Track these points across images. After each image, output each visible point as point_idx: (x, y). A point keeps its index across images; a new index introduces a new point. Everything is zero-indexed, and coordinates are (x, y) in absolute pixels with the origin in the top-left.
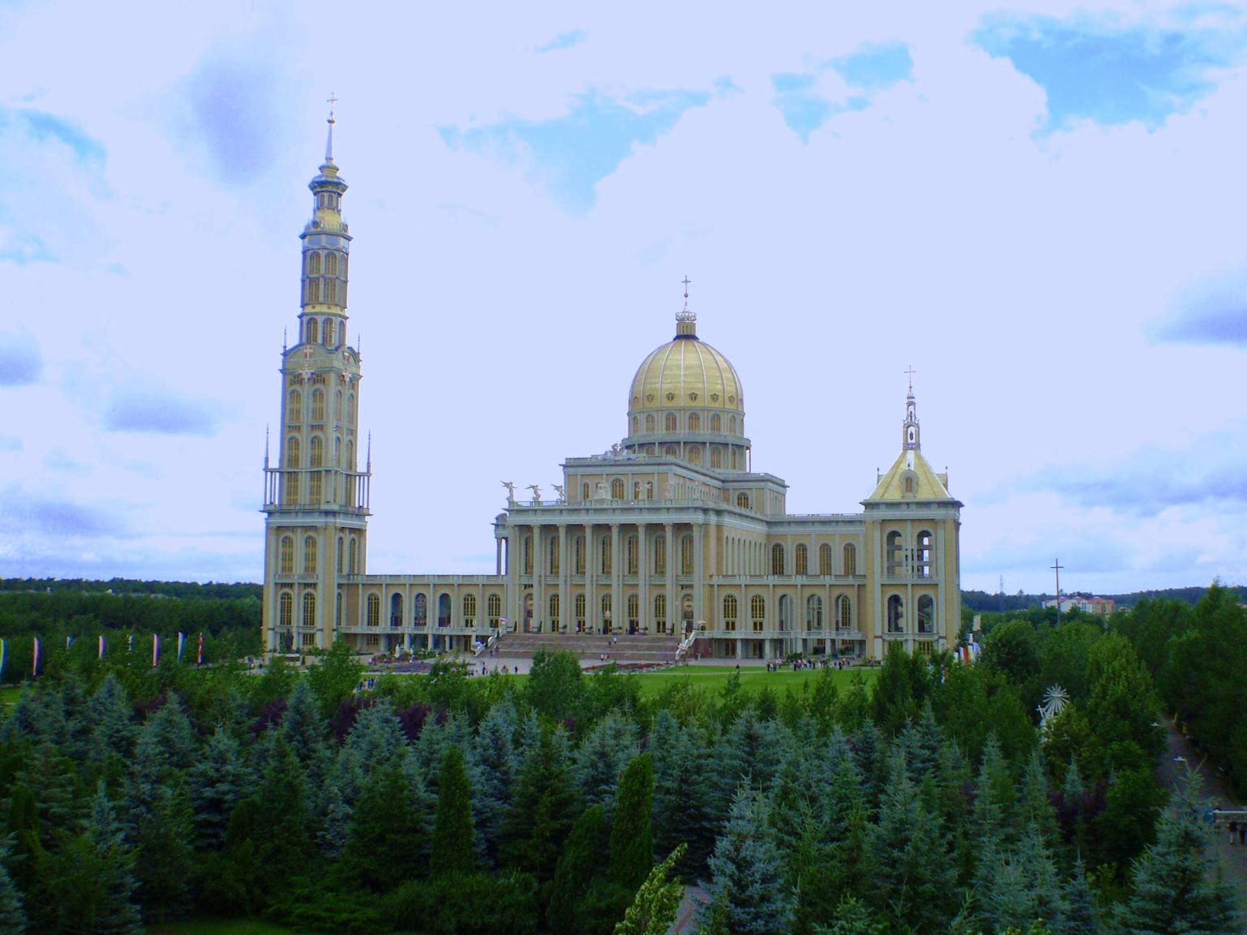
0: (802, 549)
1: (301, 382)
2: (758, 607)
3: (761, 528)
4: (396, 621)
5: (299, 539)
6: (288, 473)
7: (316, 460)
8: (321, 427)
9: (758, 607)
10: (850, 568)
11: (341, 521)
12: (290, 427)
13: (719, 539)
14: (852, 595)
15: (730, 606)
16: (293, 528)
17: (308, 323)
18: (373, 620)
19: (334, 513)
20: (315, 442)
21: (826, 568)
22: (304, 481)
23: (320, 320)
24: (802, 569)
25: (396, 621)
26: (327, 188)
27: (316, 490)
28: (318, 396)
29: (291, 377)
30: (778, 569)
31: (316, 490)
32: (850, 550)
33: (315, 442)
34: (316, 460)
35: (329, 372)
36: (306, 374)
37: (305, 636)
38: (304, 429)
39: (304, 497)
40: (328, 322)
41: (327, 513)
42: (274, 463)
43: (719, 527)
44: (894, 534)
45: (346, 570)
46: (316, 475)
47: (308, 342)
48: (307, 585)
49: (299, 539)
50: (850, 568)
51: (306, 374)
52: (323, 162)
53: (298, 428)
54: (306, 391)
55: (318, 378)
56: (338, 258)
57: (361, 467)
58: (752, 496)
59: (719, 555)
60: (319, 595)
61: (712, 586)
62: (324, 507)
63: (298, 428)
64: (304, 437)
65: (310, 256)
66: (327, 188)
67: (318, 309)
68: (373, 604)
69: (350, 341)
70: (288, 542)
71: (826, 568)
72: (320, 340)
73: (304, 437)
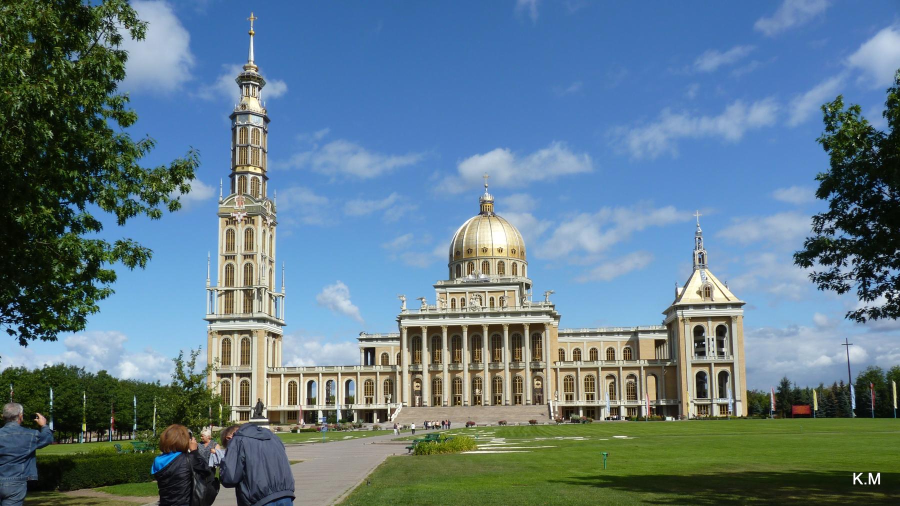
4: (311, 401)
5: (236, 341)
7: (248, 280)
8: (252, 257)
16: (231, 332)
18: (293, 400)
19: (264, 320)
20: (248, 269)
22: (239, 298)
28: (249, 233)
33: (248, 269)
35: (257, 215)
36: (239, 217)
37: (241, 413)
38: (239, 258)
45: (270, 365)
48: (241, 375)
49: (236, 341)
53: (233, 257)
54: (240, 231)
55: (249, 219)
61: (555, 370)
62: (256, 315)
63: (233, 257)
64: (239, 265)
68: (293, 388)
70: (226, 344)
72: (249, 192)
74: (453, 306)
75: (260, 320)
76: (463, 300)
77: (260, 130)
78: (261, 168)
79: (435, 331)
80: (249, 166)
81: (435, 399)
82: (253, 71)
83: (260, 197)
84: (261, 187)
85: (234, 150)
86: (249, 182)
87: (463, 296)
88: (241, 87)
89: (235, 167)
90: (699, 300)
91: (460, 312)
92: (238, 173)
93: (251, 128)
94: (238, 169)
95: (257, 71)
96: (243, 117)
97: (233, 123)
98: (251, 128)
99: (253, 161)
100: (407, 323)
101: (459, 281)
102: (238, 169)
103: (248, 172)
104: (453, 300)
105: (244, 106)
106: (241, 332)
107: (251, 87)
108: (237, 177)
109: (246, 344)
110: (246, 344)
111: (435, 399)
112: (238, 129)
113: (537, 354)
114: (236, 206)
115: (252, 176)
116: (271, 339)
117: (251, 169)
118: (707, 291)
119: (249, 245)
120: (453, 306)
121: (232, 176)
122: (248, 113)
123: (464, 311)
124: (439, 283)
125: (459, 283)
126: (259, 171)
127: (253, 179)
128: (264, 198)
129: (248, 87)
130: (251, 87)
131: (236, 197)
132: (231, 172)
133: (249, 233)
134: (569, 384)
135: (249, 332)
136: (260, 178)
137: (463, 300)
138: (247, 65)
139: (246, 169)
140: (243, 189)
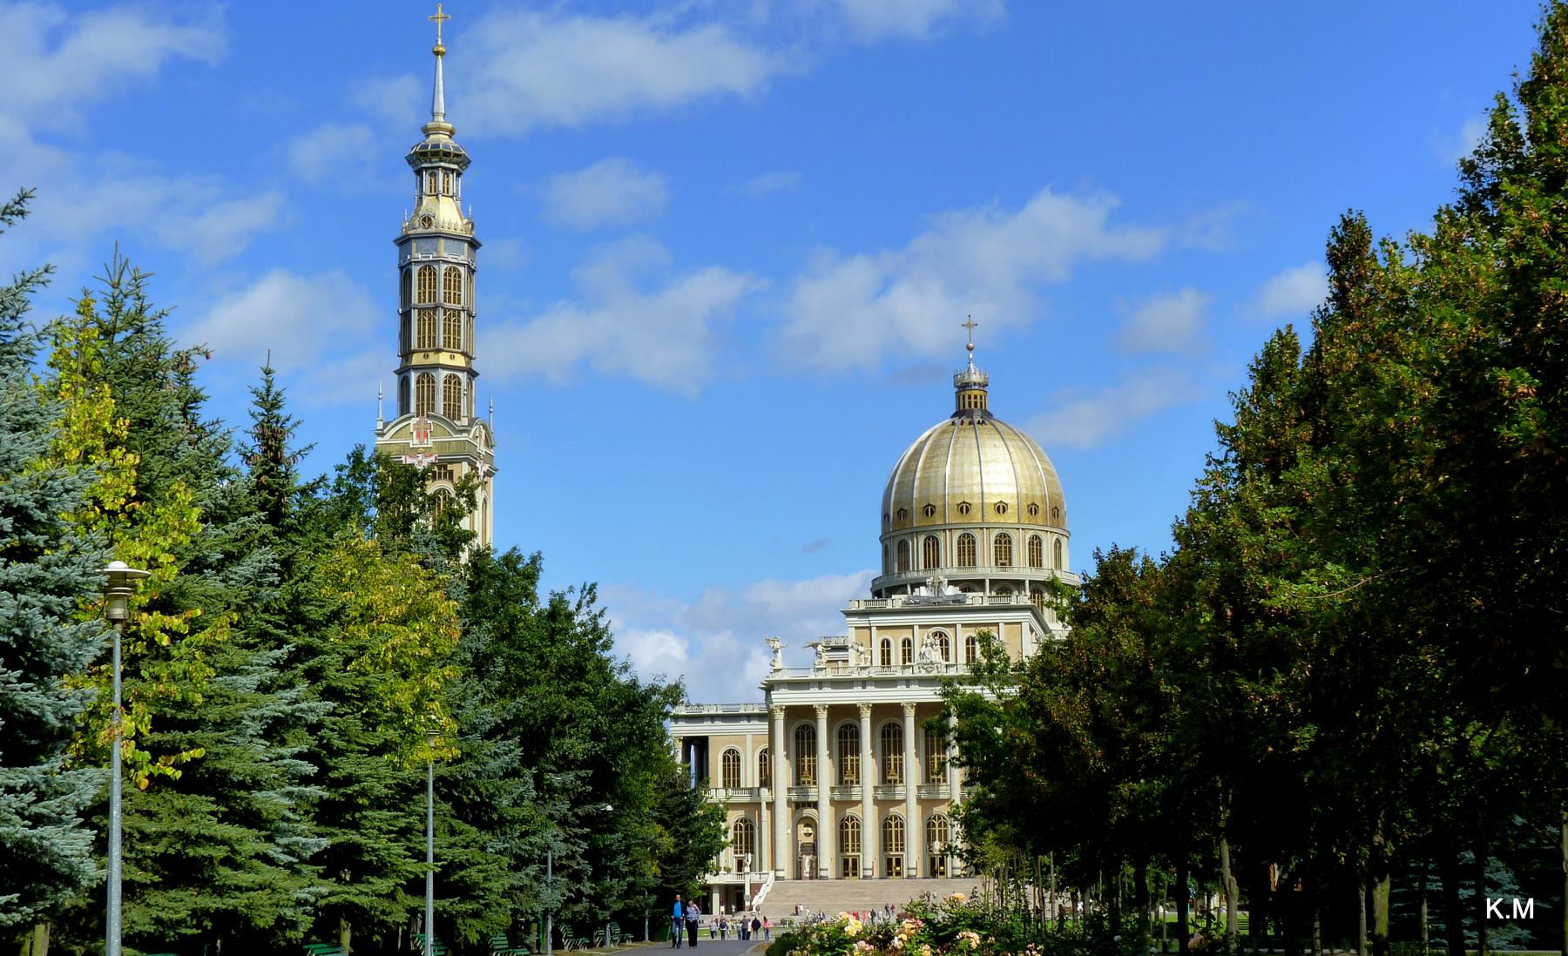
35: (459, 461)
72: (440, 410)
76: (907, 643)
77: (462, 269)
78: (463, 354)
79: (844, 717)
80: (439, 351)
81: (846, 862)
82: (443, 139)
83: (465, 421)
84: (464, 401)
85: (406, 317)
86: (440, 386)
87: (907, 634)
88: (419, 172)
89: (406, 354)
91: (899, 674)
92: (416, 368)
93: (444, 267)
94: (417, 359)
95: (451, 133)
96: (425, 244)
97: (402, 256)
98: (444, 267)
99: (447, 343)
100: (783, 698)
101: (897, 601)
102: (417, 359)
103: (437, 367)
104: (886, 644)
105: (427, 220)
107: (441, 174)
108: (414, 376)
111: (846, 862)
112: (415, 270)
114: (414, 442)
115: (445, 373)
117: (444, 358)
121: (403, 373)
122: (437, 236)
123: (908, 673)
124: (854, 607)
125: (898, 605)
126: (460, 361)
127: (448, 380)
128: (472, 422)
129: (433, 175)
130: (441, 174)
131: (414, 421)
132: (397, 363)
136: (463, 376)
137: (907, 643)
138: (430, 125)
139: (433, 359)
140: (427, 407)
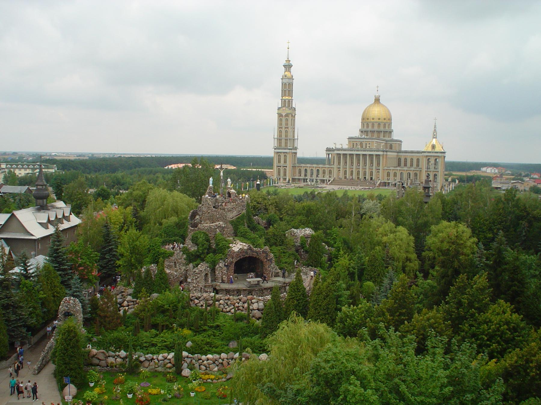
0: (406, 160)
1: (282, 116)
2: (395, 175)
3: (396, 154)
4: (305, 175)
6: (279, 140)
7: (286, 136)
9: (395, 175)
10: (418, 165)
11: (293, 151)
12: (280, 127)
13: (386, 158)
14: (418, 173)
15: (388, 174)
17: (284, 102)
19: (291, 149)
20: (286, 132)
21: (412, 165)
23: (287, 101)
24: (405, 165)
25: (305, 175)
26: (288, 67)
27: (286, 143)
28: (287, 120)
29: (280, 115)
30: (399, 165)
31: (286, 143)
32: (418, 160)
33: (286, 132)
34: (286, 136)
36: (284, 115)
38: (283, 128)
39: (283, 145)
40: (289, 101)
41: (290, 149)
42: (276, 137)
43: (386, 155)
44: (436, 159)
46: (286, 140)
47: (285, 106)
50: (418, 165)
51: (284, 115)
52: (286, 59)
54: (284, 119)
55: (287, 115)
56: (291, 85)
57: (296, 137)
58: (393, 145)
59: (386, 161)
60: (288, 169)
64: (283, 130)
65: (284, 85)
66: (288, 67)
67: (286, 98)
69: (294, 106)
70: (279, 156)
71: (412, 165)
73: (283, 130)
74: (353, 145)
75: (290, 149)
90: (430, 149)
94: (284, 98)
106: (284, 153)
109: (285, 156)
110: (285, 156)
113: (378, 164)
116: (294, 154)
118: (433, 147)
119: (287, 124)
120: (353, 145)
133: (287, 120)
134: (388, 174)
135: (286, 153)
